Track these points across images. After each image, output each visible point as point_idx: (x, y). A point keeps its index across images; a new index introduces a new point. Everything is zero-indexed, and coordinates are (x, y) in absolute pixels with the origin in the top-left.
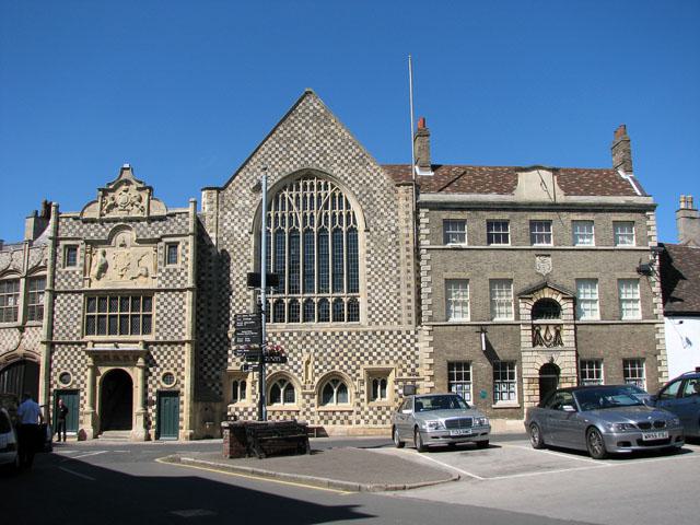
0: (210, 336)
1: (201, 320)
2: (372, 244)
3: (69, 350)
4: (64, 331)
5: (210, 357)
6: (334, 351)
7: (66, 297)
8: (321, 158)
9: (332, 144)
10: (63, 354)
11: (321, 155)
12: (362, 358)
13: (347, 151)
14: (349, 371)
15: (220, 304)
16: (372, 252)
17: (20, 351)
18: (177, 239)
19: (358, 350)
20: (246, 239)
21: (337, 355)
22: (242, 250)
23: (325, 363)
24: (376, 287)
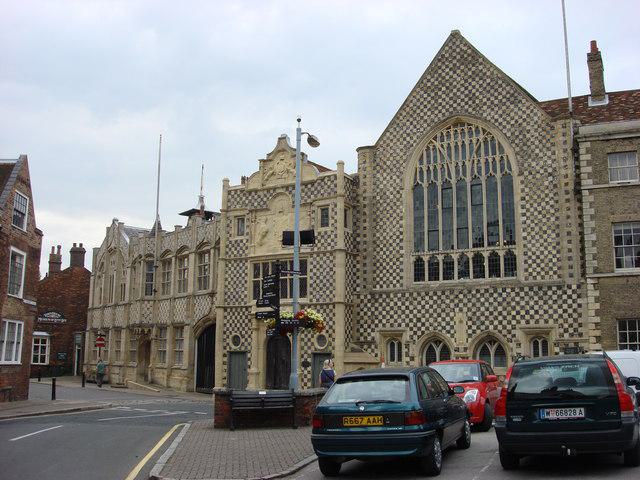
0: (366, 296)
1: (358, 281)
2: (527, 190)
5: (366, 318)
6: (487, 309)
8: (470, 102)
9: (481, 86)
11: (470, 99)
12: (518, 317)
13: (496, 90)
14: (504, 332)
15: (375, 265)
16: (527, 198)
18: (328, 202)
19: (514, 308)
20: (398, 196)
21: (491, 313)
22: (395, 208)
23: (478, 323)
24: (533, 238)
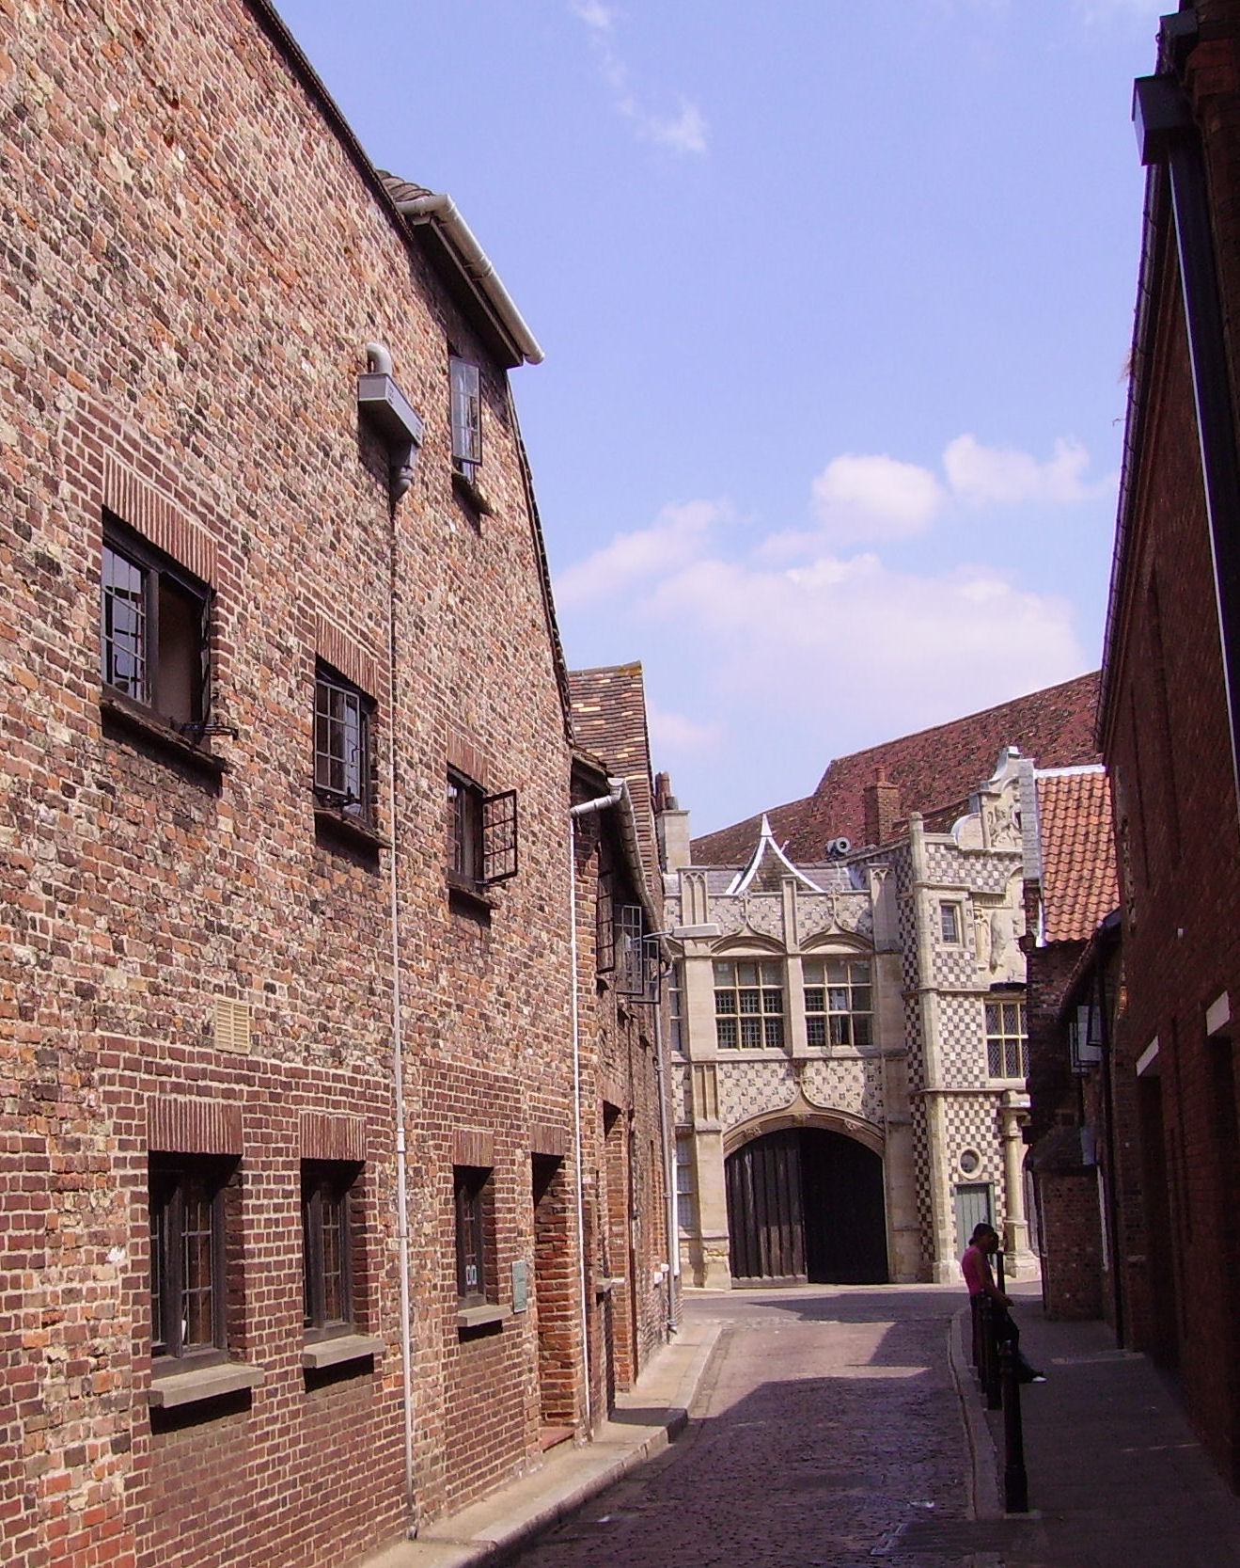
3: (972, 1106)
4: (959, 1071)
7: (955, 1004)
10: (962, 1114)
17: (800, 1110)
